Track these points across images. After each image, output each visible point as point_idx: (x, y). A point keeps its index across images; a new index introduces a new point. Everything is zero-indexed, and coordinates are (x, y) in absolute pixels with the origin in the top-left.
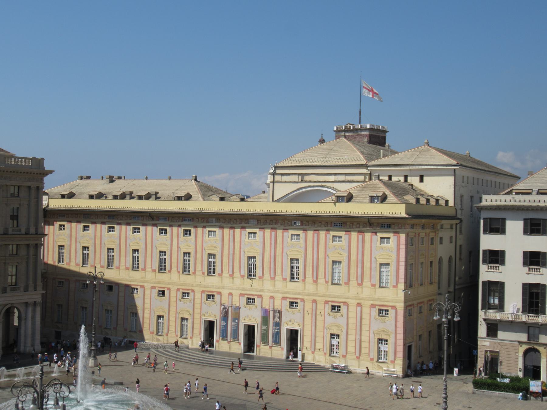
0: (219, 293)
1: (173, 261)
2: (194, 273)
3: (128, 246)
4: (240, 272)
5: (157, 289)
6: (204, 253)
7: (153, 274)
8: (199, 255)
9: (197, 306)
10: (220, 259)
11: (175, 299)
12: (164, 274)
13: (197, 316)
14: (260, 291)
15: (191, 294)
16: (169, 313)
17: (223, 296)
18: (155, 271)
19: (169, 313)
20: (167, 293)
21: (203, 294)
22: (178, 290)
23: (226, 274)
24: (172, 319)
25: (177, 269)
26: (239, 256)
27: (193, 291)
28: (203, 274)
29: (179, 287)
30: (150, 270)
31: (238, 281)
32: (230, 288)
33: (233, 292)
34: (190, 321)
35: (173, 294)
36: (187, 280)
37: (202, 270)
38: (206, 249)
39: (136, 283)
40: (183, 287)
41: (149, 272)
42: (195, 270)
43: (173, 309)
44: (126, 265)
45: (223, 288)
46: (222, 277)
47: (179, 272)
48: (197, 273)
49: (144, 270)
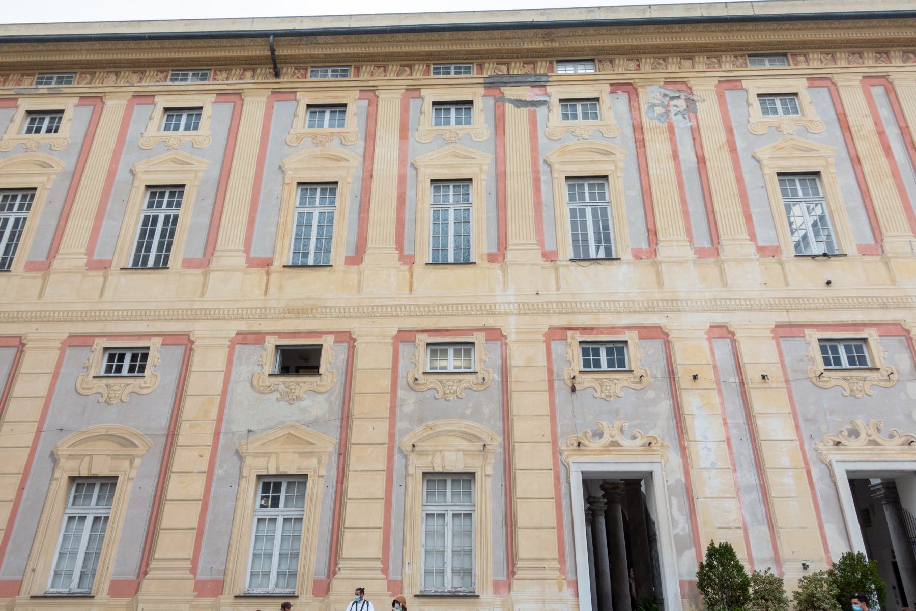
0: (653, 333)
1: (375, 214)
2: (497, 257)
3: (122, 174)
4: (753, 237)
5: (271, 342)
6: (543, 178)
7: (257, 276)
8: (519, 187)
9: (530, 405)
10: (635, 193)
11: (385, 383)
12: (322, 273)
13: (533, 457)
14: (885, 307)
15: (484, 356)
16: (343, 452)
17: (677, 347)
18: (266, 263)
19: (343, 452)
20: (331, 359)
21: (557, 346)
22: (405, 336)
23: (675, 246)
24: (365, 485)
25: (399, 245)
26: (731, 176)
27: (495, 335)
28: (550, 257)
29: (410, 324)
30: (241, 261)
31: (748, 277)
32: (713, 306)
33: (735, 320)
34: (487, 490)
35: (373, 356)
36: (447, 295)
37: (541, 243)
38: (553, 159)
39: (142, 327)
40: (430, 323)
41: (233, 269)
42: (502, 243)
43: (369, 432)
44: (90, 250)
45: (674, 306)
46: (656, 264)
47: (408, 260)
48: (510, 255)
49: (203, 262)
